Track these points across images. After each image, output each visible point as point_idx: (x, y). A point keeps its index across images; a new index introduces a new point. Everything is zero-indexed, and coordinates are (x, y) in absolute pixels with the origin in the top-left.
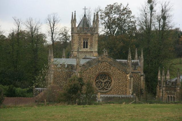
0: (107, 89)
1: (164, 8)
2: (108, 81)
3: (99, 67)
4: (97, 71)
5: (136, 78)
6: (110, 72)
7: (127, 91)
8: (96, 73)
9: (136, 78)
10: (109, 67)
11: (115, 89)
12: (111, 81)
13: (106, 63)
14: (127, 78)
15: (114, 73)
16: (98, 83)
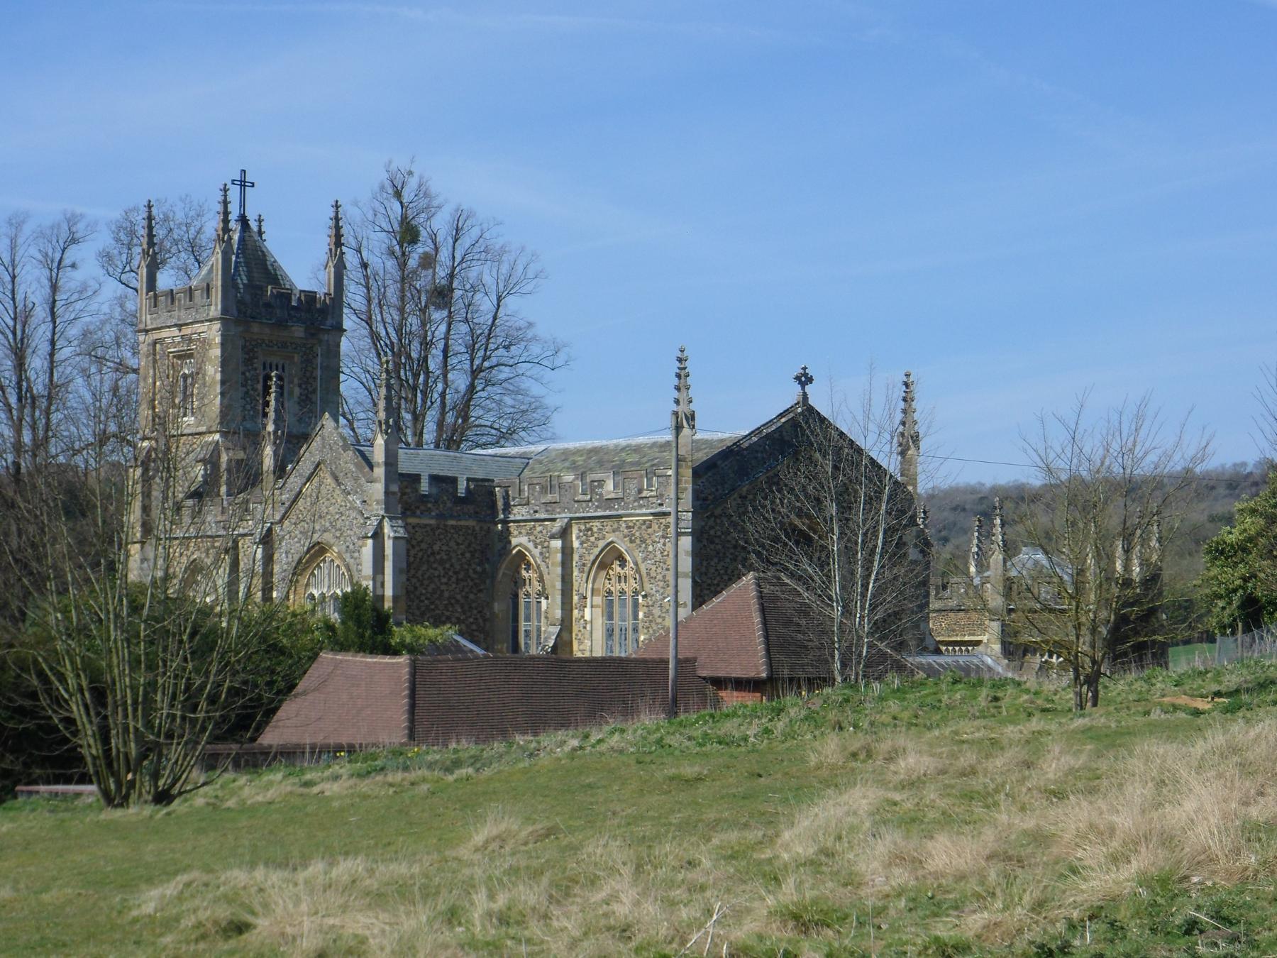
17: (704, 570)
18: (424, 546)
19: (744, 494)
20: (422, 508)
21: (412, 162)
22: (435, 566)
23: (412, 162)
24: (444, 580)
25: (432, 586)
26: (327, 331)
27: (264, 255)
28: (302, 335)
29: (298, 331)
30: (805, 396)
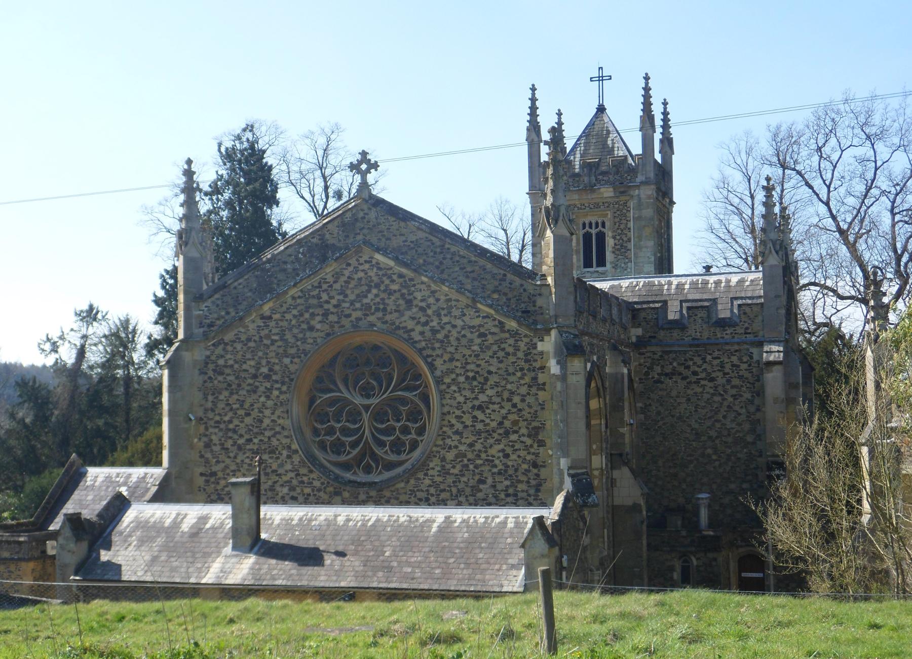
0: (393, 457)
2: (403, 401)
3: (325, 297)
4: (315, 323)
5: (736, 382)
6: (410, 324)
7: (544, 473)
9: (736, 382)
10: (395, 287)
11: (450, 456)
12: (426, 399)
13: (378, 257)
14: (542, 368)
15: (434, 332)
16: (327, 414)
17: (209, 405)
19: (268, 313)
26: (638, 187)
28: (612, 194)
29: (607, 192)
30: (364, 185)
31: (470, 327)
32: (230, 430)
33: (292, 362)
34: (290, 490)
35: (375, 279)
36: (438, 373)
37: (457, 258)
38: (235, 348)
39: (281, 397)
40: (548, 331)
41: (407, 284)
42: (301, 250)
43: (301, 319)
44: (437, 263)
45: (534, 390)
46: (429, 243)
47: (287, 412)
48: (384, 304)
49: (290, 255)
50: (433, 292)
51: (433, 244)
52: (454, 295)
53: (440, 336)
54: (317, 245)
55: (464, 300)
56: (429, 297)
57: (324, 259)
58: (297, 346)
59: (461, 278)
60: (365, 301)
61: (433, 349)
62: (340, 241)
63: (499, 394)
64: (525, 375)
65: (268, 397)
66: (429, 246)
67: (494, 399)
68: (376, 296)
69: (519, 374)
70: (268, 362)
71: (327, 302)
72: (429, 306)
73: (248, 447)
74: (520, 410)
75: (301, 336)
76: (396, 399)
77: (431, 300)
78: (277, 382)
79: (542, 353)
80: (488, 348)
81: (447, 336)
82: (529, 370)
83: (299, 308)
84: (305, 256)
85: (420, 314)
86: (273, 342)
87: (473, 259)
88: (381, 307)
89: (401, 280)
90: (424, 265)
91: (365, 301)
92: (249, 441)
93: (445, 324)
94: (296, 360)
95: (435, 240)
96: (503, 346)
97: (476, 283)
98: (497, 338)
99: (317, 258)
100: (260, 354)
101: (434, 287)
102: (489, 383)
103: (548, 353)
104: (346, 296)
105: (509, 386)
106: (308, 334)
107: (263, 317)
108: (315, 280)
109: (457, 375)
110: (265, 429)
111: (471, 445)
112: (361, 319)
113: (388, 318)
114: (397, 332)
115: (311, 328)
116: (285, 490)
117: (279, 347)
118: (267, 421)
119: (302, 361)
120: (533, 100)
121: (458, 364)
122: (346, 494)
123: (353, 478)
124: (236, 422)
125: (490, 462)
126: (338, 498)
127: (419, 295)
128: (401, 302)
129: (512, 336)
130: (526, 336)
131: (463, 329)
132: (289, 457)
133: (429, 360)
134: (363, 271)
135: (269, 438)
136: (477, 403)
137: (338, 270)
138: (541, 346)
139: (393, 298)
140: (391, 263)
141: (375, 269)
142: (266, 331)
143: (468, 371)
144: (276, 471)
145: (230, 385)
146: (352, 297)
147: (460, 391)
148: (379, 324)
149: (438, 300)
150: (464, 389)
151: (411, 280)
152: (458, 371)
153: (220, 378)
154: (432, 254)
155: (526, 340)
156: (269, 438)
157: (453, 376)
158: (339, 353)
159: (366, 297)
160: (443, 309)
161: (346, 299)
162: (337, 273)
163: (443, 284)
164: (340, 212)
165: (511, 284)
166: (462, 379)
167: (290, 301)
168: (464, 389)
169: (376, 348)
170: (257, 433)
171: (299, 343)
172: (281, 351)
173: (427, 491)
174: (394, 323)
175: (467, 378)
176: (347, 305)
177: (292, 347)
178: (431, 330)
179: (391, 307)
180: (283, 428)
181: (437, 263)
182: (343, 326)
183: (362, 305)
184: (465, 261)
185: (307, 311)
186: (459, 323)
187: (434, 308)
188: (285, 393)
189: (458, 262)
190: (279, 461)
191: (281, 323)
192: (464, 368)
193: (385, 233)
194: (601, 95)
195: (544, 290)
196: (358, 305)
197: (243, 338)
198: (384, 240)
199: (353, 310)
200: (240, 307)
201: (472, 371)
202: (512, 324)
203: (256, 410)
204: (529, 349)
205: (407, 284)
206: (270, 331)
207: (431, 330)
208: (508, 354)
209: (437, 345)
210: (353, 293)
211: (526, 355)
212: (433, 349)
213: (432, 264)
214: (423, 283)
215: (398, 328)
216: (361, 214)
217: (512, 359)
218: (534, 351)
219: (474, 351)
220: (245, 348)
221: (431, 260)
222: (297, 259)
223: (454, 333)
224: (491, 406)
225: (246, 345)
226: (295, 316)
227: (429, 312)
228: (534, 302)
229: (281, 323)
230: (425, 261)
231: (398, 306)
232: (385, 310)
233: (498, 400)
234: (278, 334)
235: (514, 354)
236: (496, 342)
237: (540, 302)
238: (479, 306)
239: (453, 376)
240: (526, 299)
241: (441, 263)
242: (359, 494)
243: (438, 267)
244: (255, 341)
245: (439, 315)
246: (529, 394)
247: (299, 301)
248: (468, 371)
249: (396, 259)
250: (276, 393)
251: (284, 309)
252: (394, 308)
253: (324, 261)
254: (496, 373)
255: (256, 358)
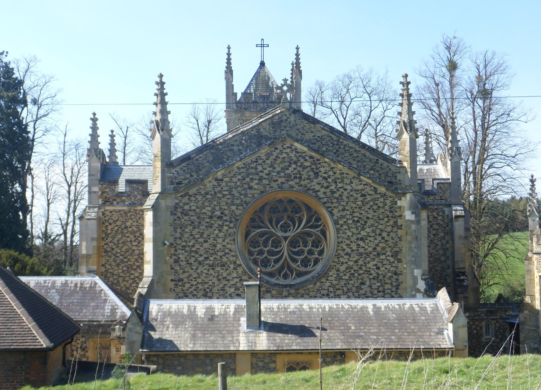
0: (303, 269)
1: (481, 67)
2: (309, 234)
3: (260, 168)
4: (254, 184)
5: (435, 227)
6: (317, 187)
7: (401, 278)
8: (246, 195)
9: (435, 227)
11: (343, 268)
12: (324, 233)
14: (400, 216)
15: (333, 192)
16: (257, 242)
17: (178, 235)
18: (119, 223)
19: (220, 177)
20: (118, 200)
21: (455, 32)
22: (127, 235)
23: (455, 32)
24: (134, 244)
25: (126, 247)
27: (269, 78)
31: (355, 190)
32: (193, 251)
33: (237, 209)
34: (235, 290)
35: (295, 159)
36: (335, 218)
37: (348, 148)
38: (197, 199)
39: (230, 231)
40: (404, 194)
41: (315, 162)
42: (244, 138)
43: (244, 182)
44: (335, 151)
45: (395, 229)
46: (330, 138)
47: (234, 240)
48: (300, 174)
49: (236, 141)
50: (332, 168)
51: (332, 139)
52: (346, 170)
53: (336, 195)
54: (255, 135)
55: (352, 174)
56: (329, 171)
57: (259, 145)
58: (241, 199)
59: (350, 160)
60: (287, 172)
61: (332, 203)
62: (270, 133)
63: (373, 231)
64: (389, 220)
65: (220, 231)
66: (329, 140)
67: (371, 234)
68: (295, 169)
69: (386, 219)
70: (220, 209)
71: (262, 172)
72: (329, 177)
73: (206, 262)
74: (386, 241)
75: (243, 192)
76: (304, 233)
77: (331, 173)
78: (226, 221)
79: (400, 207)
80: (367, 203)
81: (341, 196)
82: (392, 217)
83: (242, 175)
84: (247, 142)
85: (324, 181)
86: (224, 196)
87: (358, 149)
88: (298, 176)
89: (312, 160)
90: (326, 151)
91: (287, 172)
92: (207, 258)
93: (340, 188)
94: (240, 207)
95: (333, 136)
96: (376, 202)
97: (360, 164)
98: (372, 197)
99: (255, 143)
100: (215, 203)
101: (333, 165)
102: (367, 225)
103: (404, 207)
104: (274, 168)
105: (380, 227)
106: (248, 191)
107: (216, 180)
108: (253, 158)
109: (347, 219)
110: (218, 251)
111: (356, 262)
112: (284, 183)
113: (302, 183)
114: (308, 192)
115: (251, 188)
116: (232, 290)
117: (228, 199)
118: (219, 246)
119: (244, 208)
120: (229, 54)
121: (348, 213)
122: (274, 292)
123: (277, 282)
124: (197, 246)
125: (368, 272)
126: (269, 295)
127: (323, 170)
128: (311, 173)
129: (382, 197)
130: (390, 197)
131: (351, 191)
132: (235, 269)
133: (330, 209)
134: (286, 153)
135: (221, 257)
136: (360, 236)
137: (269, 152)
138: (399, 203)
139: (306, 171)
140: (306, 149)
141: (294, 152)
142: (219, 189)
143: (354, 217)
144: (226, 278)
145: (193, 222)
146: (279, 169)
147: (349, 229)
148: (297, 187)
149: (335, 173)
150: (352, 228)
151: (318, 160)
152: (348, 217)
153: (186, 218)
154: (332, 145)
155: (391, 199)
156: (221, 257)
157: (345, 220)
158: (266, 204)
159: (288, 169)
160: (338, 179)
161: (274, 170)
162: (268, 154)
163: (340, 164)
164: (271, 116)
165: (381, 165)
166: (350, 222)
167: (236, 170)
168: (352, 228)
169: (291, 201)
170: (212, 254)
171: (242, 197)
172: (229, 201)
173: (328, 289)
174: (306, 186)
175: (354, 221)
176: (275, 174)
177: (237, 199)
178: (330, 191)
179: (305, 176)
180: (230, 250)
181: (335, 151)
182: (272, 187)
183: (285, 174)
184: (352, 150)
185: (248, 177)
186: (349, 187)
187: (333, 178)
188: (232, 228)
189: (348, 150)
190: (228, 272)
191: (229, 184)
192: (352, 215)
193: (301, 130)
194: (262, 55)
195: (402, 170)
196: (282, 174)
197: (203, 192)
198: (300, 134)
199: (279, 177)
200: (200, 172)
201: (357, 217)
202: (382, 190)
203: (212, 239)
204: (392, 205)
205: (315, 162)
206: (222, 188)
207: (330, 191)
208: (379, 207)
209: (335, 201)
210: (279, 166)
211: (390, 208)
212: (332, 203)
213: (332, 151)
214: (325, 162)
215: (309, 189)
216: (285, 118)
217: (382, 210)
218: (395, 206)
219: (358, 205)
220: (204, 199)
221: (331, 148)
222: (241, 143)
223: (345, 193)
224: (369, 238)
225: (204, 197)
226: (239, 180)
227: (330, 180)
228: (396, 177)
229: (229, 184)
230: (327, 149)
231: (309, 176)
232: (300, 178)
233: (373, 234)
234: (227, 190)
235: (383, 207)
236: (372, 200)
237: (399, 177)
238: (362, 177)
239: (345, 220)
240: (391, 175)
241: (337, 151)
242: (283, 292)
243: (335, 153)
244: (211, 194)
245: (336, 182)
246: (392, 231)
247: (242, 170)
248: (354, 217)
249: (308, 147)
250: (226, 228)
251: (232, 175)
252: (307, 177)
253: (259, 146)
254: (372, 218)
255: (212, 205)
